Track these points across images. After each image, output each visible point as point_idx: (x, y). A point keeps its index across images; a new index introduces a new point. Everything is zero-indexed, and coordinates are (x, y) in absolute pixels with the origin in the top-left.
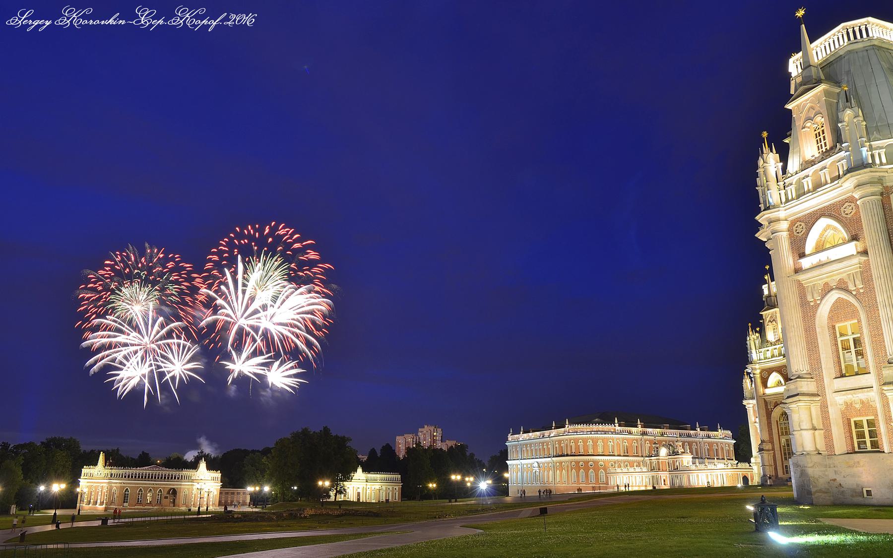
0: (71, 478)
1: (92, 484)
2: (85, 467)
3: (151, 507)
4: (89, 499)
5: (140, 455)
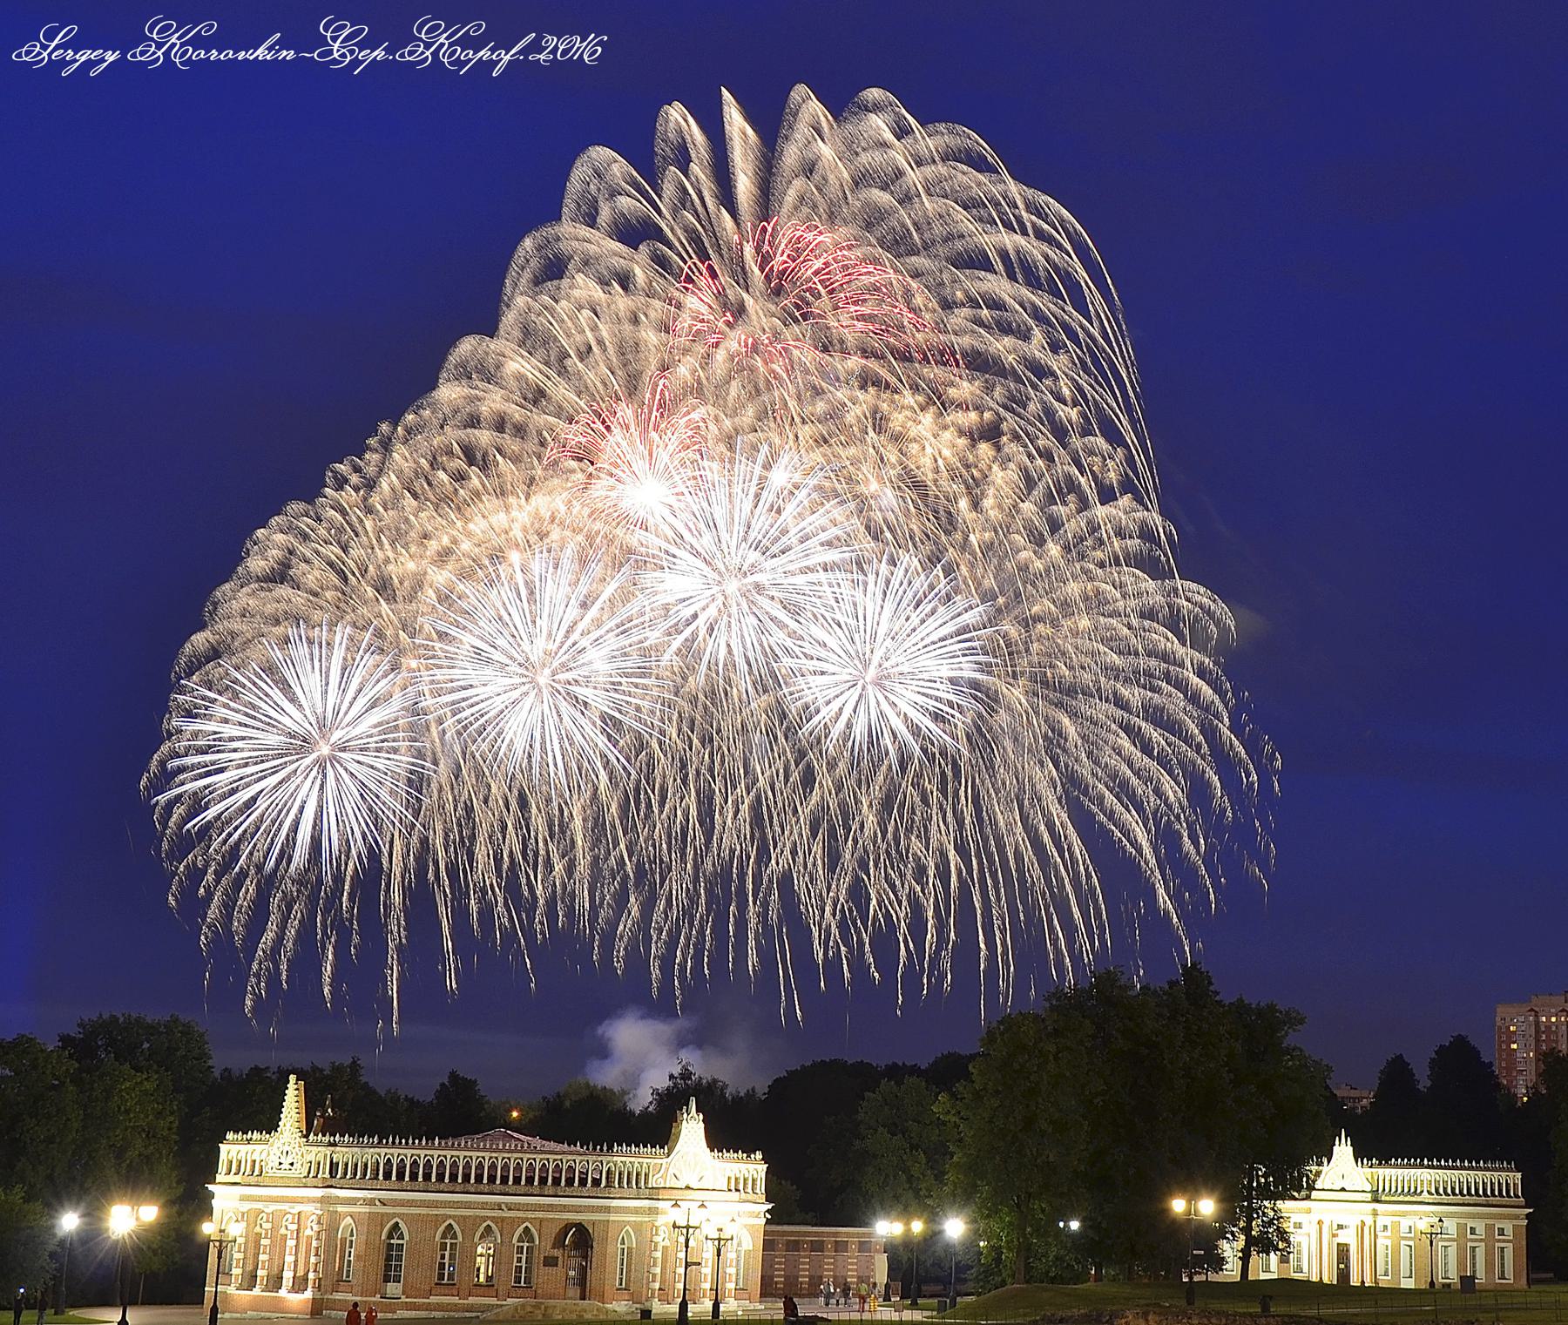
0: (178, 1183)
1: (259, 1206)
2: (230, 1136)
3: (493, 1301)
4: (249, 1268)
5: (442, 1085)
